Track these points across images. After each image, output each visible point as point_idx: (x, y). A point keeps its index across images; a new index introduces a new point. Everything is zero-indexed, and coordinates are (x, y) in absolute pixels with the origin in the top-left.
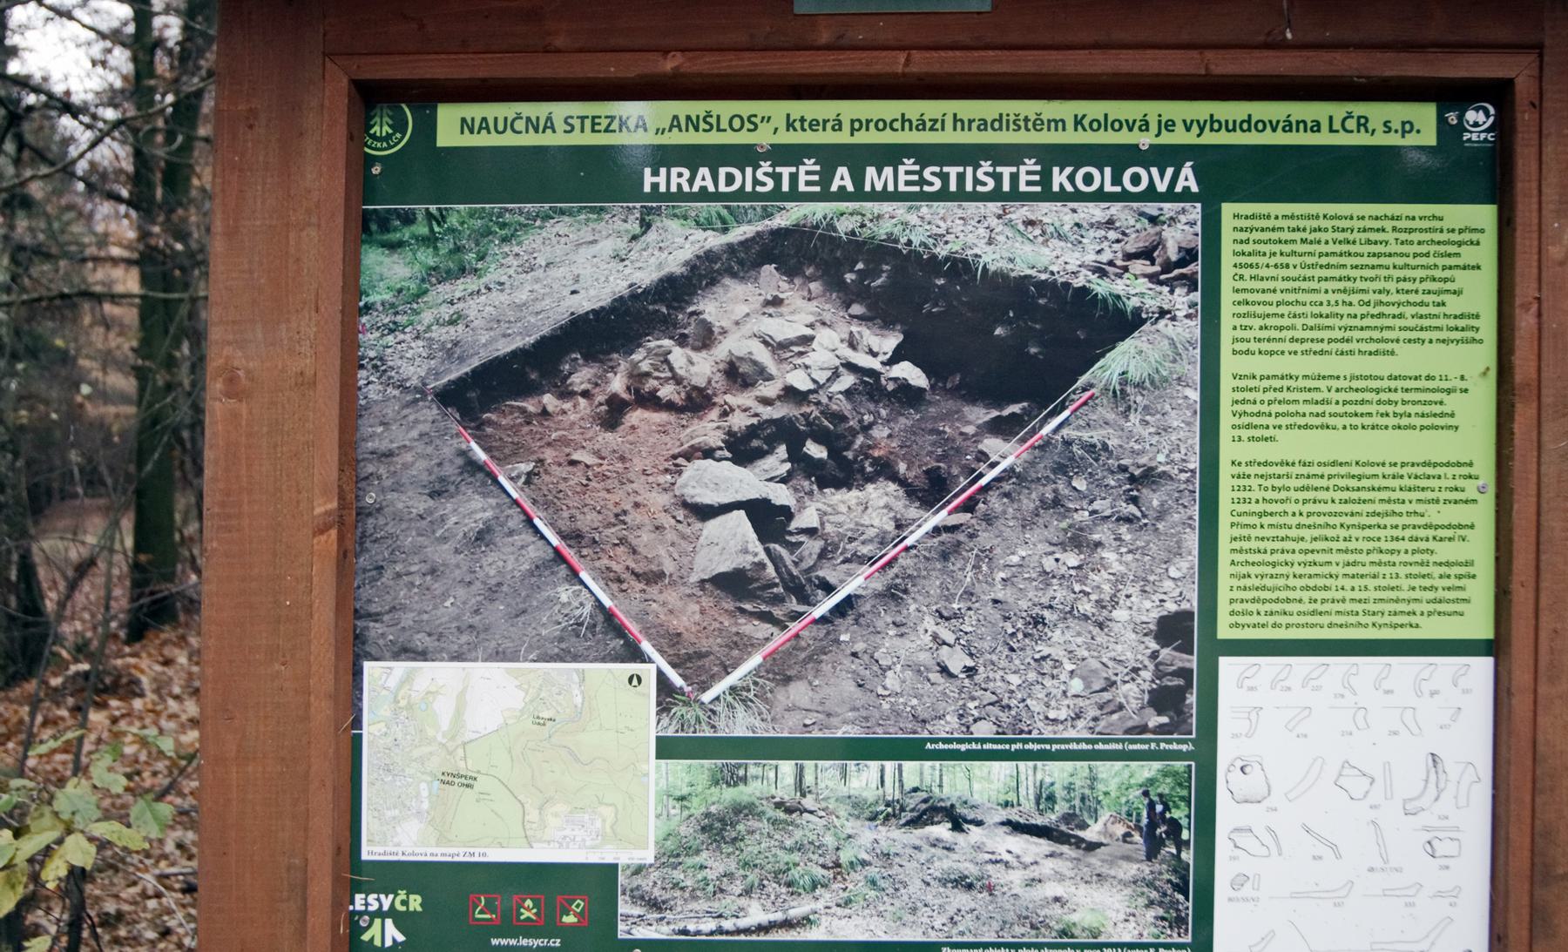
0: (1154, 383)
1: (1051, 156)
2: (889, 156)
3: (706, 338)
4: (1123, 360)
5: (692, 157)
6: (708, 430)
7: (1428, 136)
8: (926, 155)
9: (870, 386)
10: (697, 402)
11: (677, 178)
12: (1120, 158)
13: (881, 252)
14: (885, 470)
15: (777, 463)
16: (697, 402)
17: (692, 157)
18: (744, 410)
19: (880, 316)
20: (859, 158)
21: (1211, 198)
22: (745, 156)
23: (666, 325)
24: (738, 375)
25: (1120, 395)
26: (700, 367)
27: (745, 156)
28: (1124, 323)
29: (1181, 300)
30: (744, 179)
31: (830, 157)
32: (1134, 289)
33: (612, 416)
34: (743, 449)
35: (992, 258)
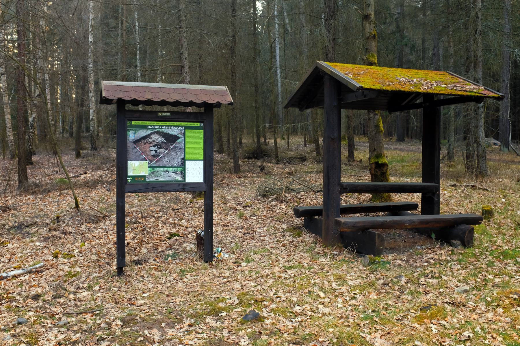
0: (181, 142)
1: (174, 126)
2: (163, 126)
3: (151, 138)
4: (179, 140)
5: (150, 126)
6: (152, 145)
7: (199, 125)
8: (166, 126)
9: (162, 142)
10: (151, 143)
11: (149, 127)
12: (179, 126)
13: (163, 133)
14: (163, 148)
15: (156, 147)
16: (151, 143)
17: (150, 126)
18: (154, 143)
19: (163, 137)
20: (161, 126)
21: (185, 129)
22: (153, 126)
23: (148, 138)
24: (154, 141)
25: (179, 143)
26: (151, 140)
27: (153, 126)
28: (179, 138)
29: (183, 136)
30: (154, 127)
31: (159, 126)
32: (180, 135)
33: (145, 144)
34: (154, 146)
35: (170, 133)
